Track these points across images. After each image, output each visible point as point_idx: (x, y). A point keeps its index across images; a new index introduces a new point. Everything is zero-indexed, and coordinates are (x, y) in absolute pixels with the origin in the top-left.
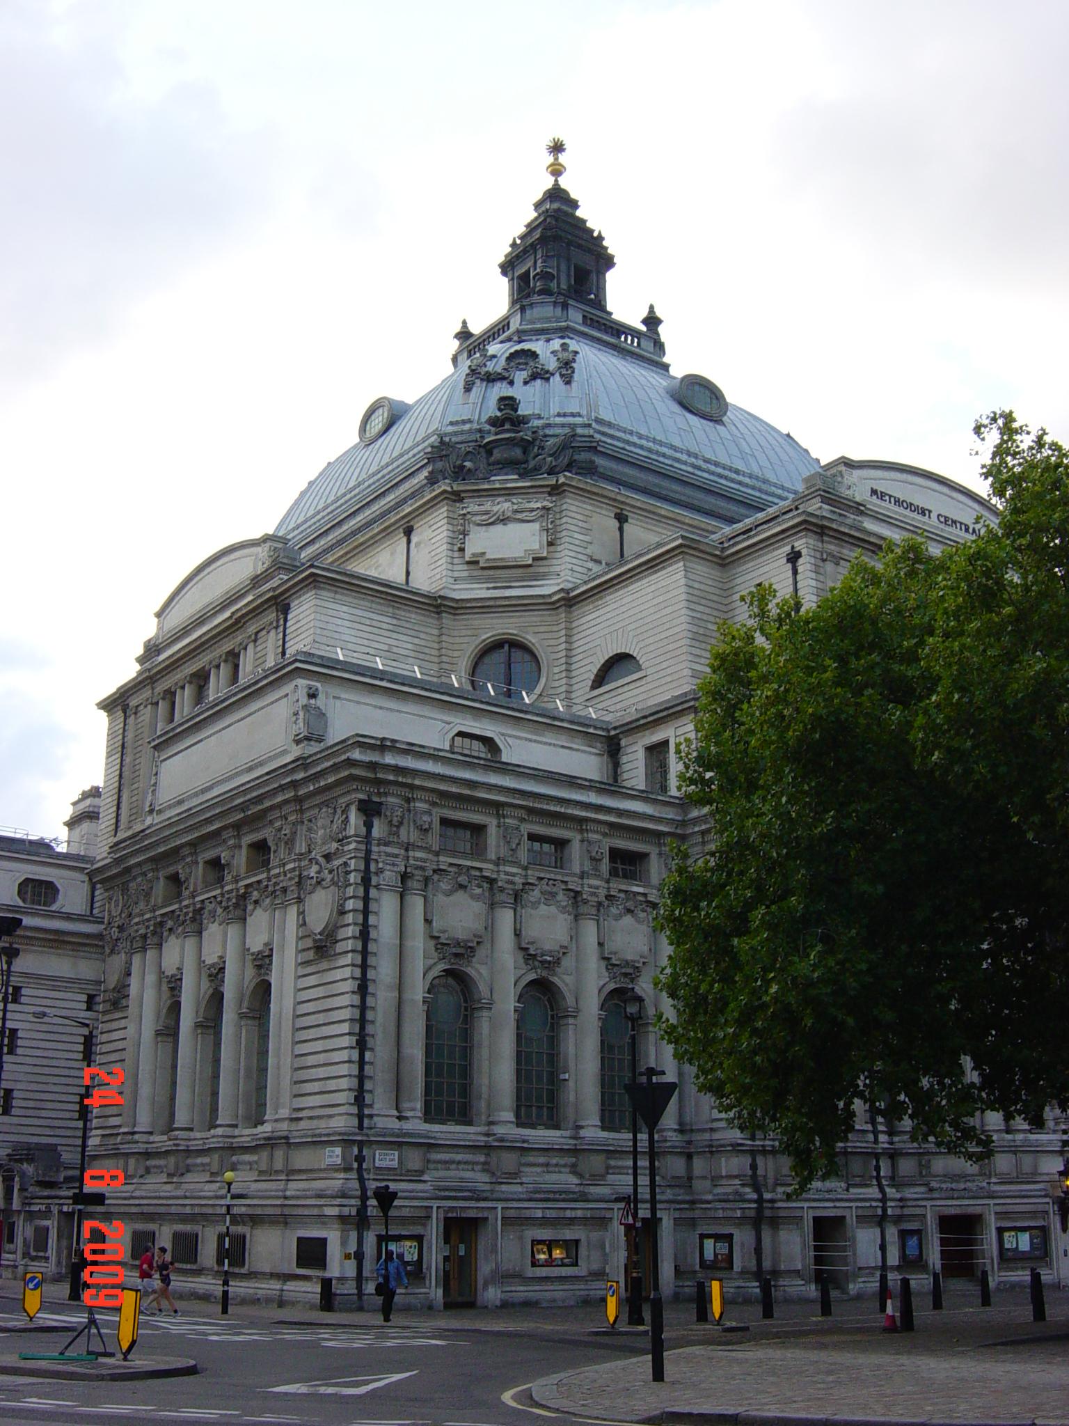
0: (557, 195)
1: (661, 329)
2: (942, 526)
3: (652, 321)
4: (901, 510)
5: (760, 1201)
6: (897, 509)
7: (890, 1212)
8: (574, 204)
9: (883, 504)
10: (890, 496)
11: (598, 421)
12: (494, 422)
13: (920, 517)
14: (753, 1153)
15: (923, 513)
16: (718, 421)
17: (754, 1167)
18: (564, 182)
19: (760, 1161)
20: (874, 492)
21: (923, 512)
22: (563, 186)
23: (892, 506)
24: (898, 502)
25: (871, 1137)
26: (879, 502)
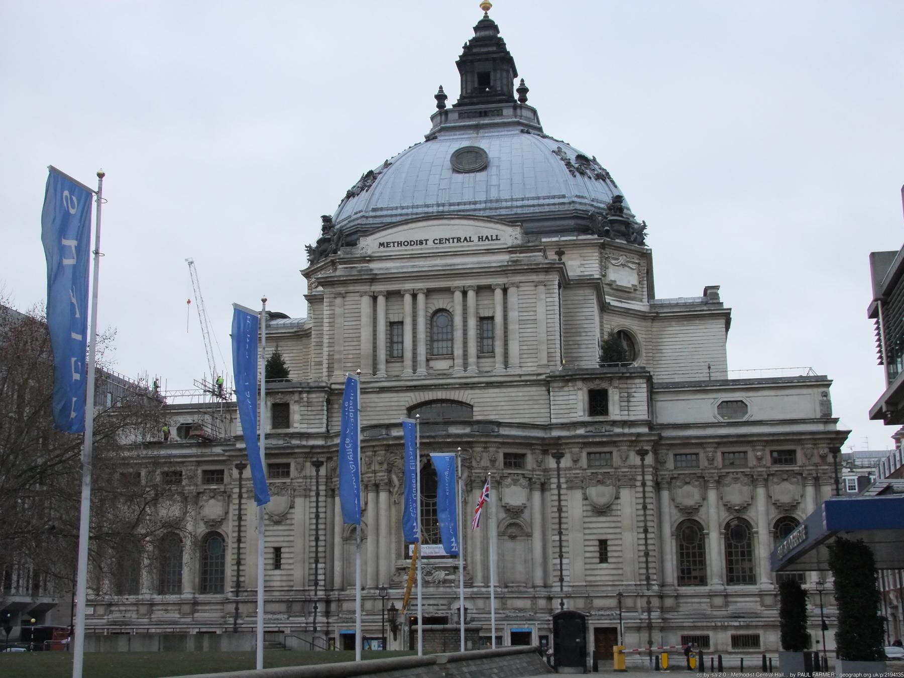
0: (486, 27)
1: (528, 95)
2: (438, 246)
3: (523, 90)
4: (404, 248)
5: (235, 624)
6: (400, 248)
7: (318, 629)
8: (495, 28)
9: (389, 249)
10: (394, 243)
11: (374, 210)
12: (324, 229)
13: (419, 247)
14: (237, 602)
15: (421, 243)
16: (484, 168)
17: (237, 609)
18: (492, 15)
19: (240, 606)
20: (381, 244)
21: (421, 243)
22: (491, 17)
23: (396, 248)
24: (400, 244)
25: (312, 593)
26: (386, 249)
